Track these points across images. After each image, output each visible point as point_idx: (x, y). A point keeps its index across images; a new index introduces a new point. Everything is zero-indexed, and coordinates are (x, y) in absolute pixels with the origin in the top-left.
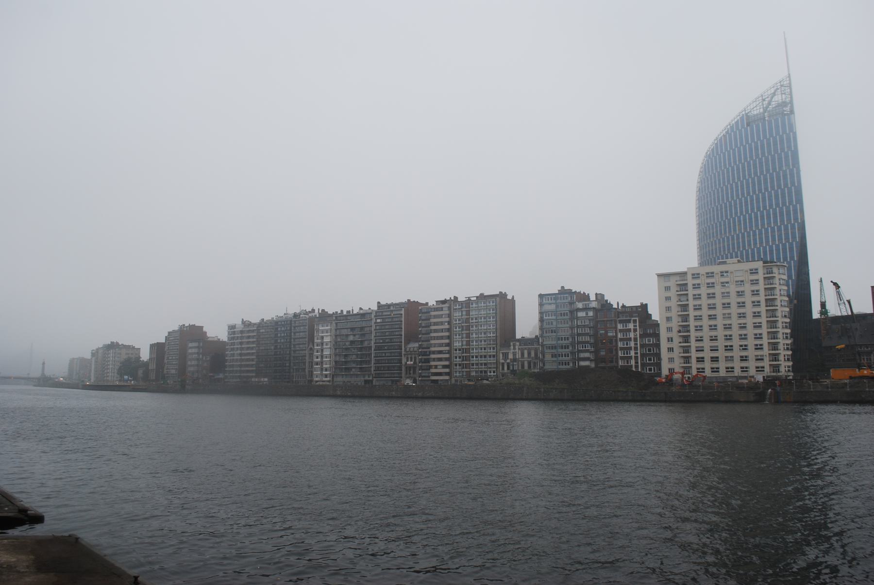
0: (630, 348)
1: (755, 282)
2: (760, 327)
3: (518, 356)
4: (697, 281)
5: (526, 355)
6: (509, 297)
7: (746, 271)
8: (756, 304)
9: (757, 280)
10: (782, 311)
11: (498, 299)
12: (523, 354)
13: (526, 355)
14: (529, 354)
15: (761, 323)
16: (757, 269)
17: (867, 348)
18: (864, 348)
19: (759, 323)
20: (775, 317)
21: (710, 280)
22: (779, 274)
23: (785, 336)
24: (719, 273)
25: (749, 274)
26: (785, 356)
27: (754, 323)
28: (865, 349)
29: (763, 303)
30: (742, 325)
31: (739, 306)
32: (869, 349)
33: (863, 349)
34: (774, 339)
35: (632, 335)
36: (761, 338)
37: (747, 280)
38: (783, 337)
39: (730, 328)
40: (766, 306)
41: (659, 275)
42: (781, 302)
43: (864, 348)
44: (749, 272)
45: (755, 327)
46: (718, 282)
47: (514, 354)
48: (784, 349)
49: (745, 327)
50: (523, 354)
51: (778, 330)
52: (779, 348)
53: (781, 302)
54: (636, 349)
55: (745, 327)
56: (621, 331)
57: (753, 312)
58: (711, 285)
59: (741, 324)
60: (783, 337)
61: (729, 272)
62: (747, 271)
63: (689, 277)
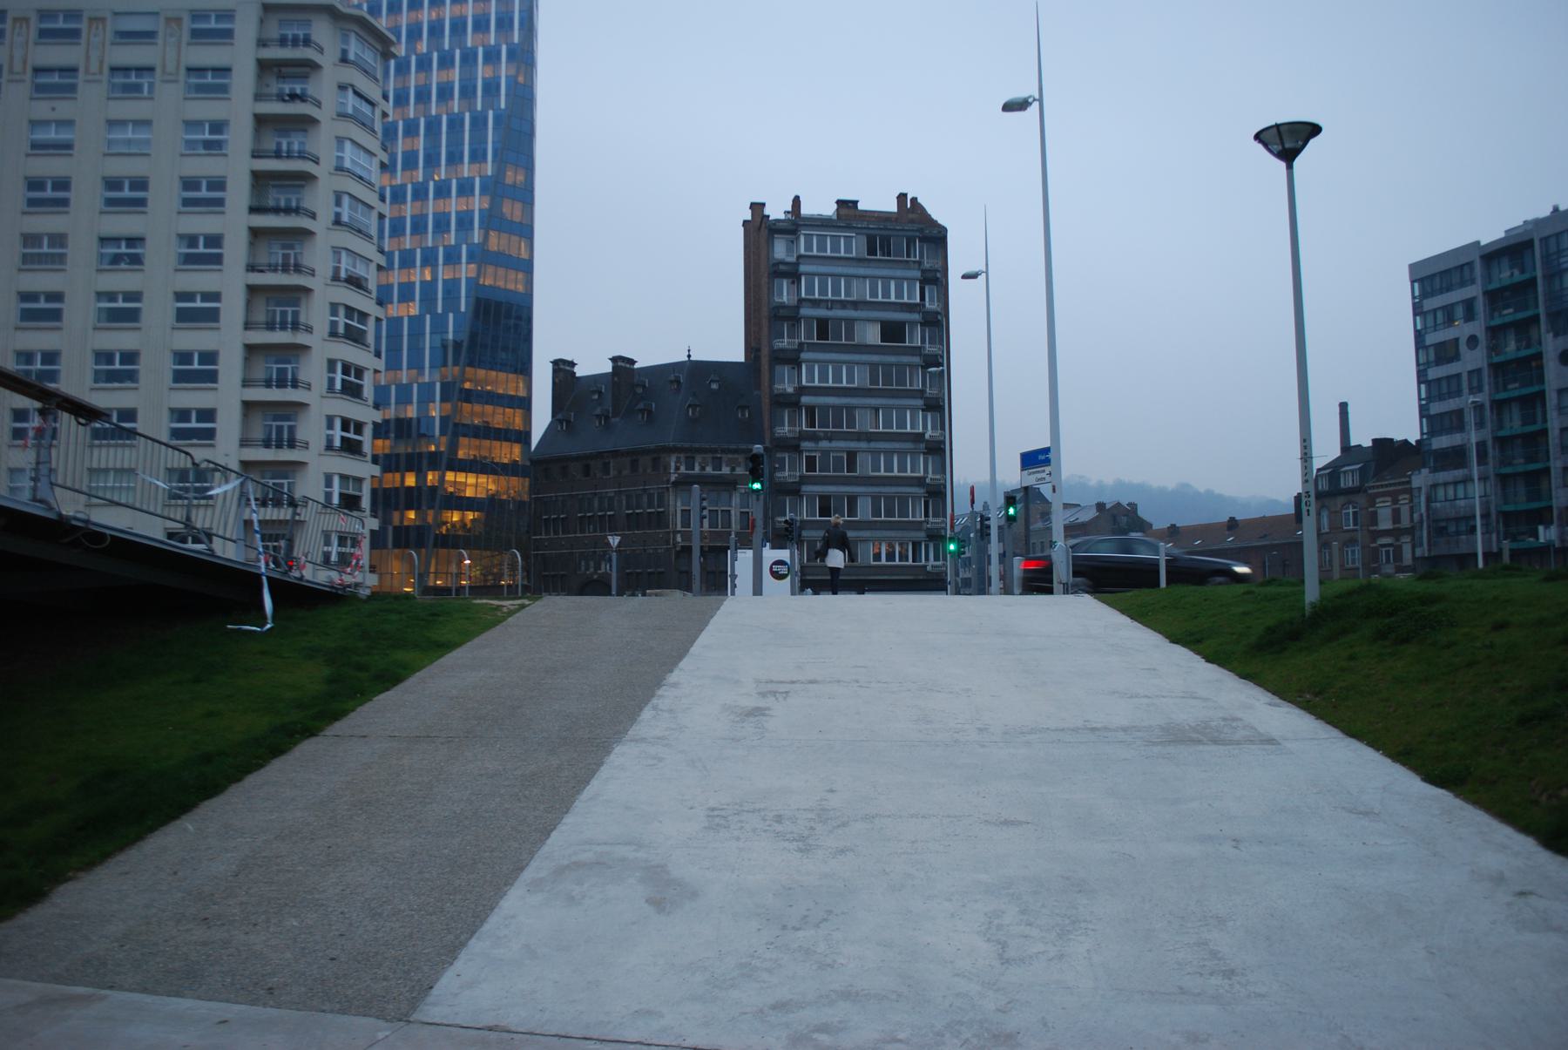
1: (210, 81)
2: (212, 316)
7: (168, 20)
8: (204, 193)
9: (225, 71)
10: (337, 251)
15: (216, 297)
16: (227, 15)
17: (718, 467)
18: (703, 468)
19: (207, 297)
20: (298, 268)
22: (344, 60)
23: (339, 377)
24: (34, 18)
25: (186, 37)
26: (329, 483)
27: (180, 296)
28: (709, 470)
29: (239, 194)
30: (121, 304)
31: (111, 202)
32: (726, 470)
33: (697, 469)
34: (281, 383)
36: (212, 377)
37: (171, 67)
38: (331, 381)
39: (56, 315)
40: (254, 210)
42: (338, 203)
43: (703, 468)
44: (187, 24)
45: (184, 316)
46: (18, 67)
48: (329, 447)
49: (132, 316)
51: (301, 338)
52: (301, 435)
53: (338, 203)
55: (132, 316)
57: (181, 237)
59: (111, 296)
60: (331, 381)
61: (86, 15)
62: (178, 20)
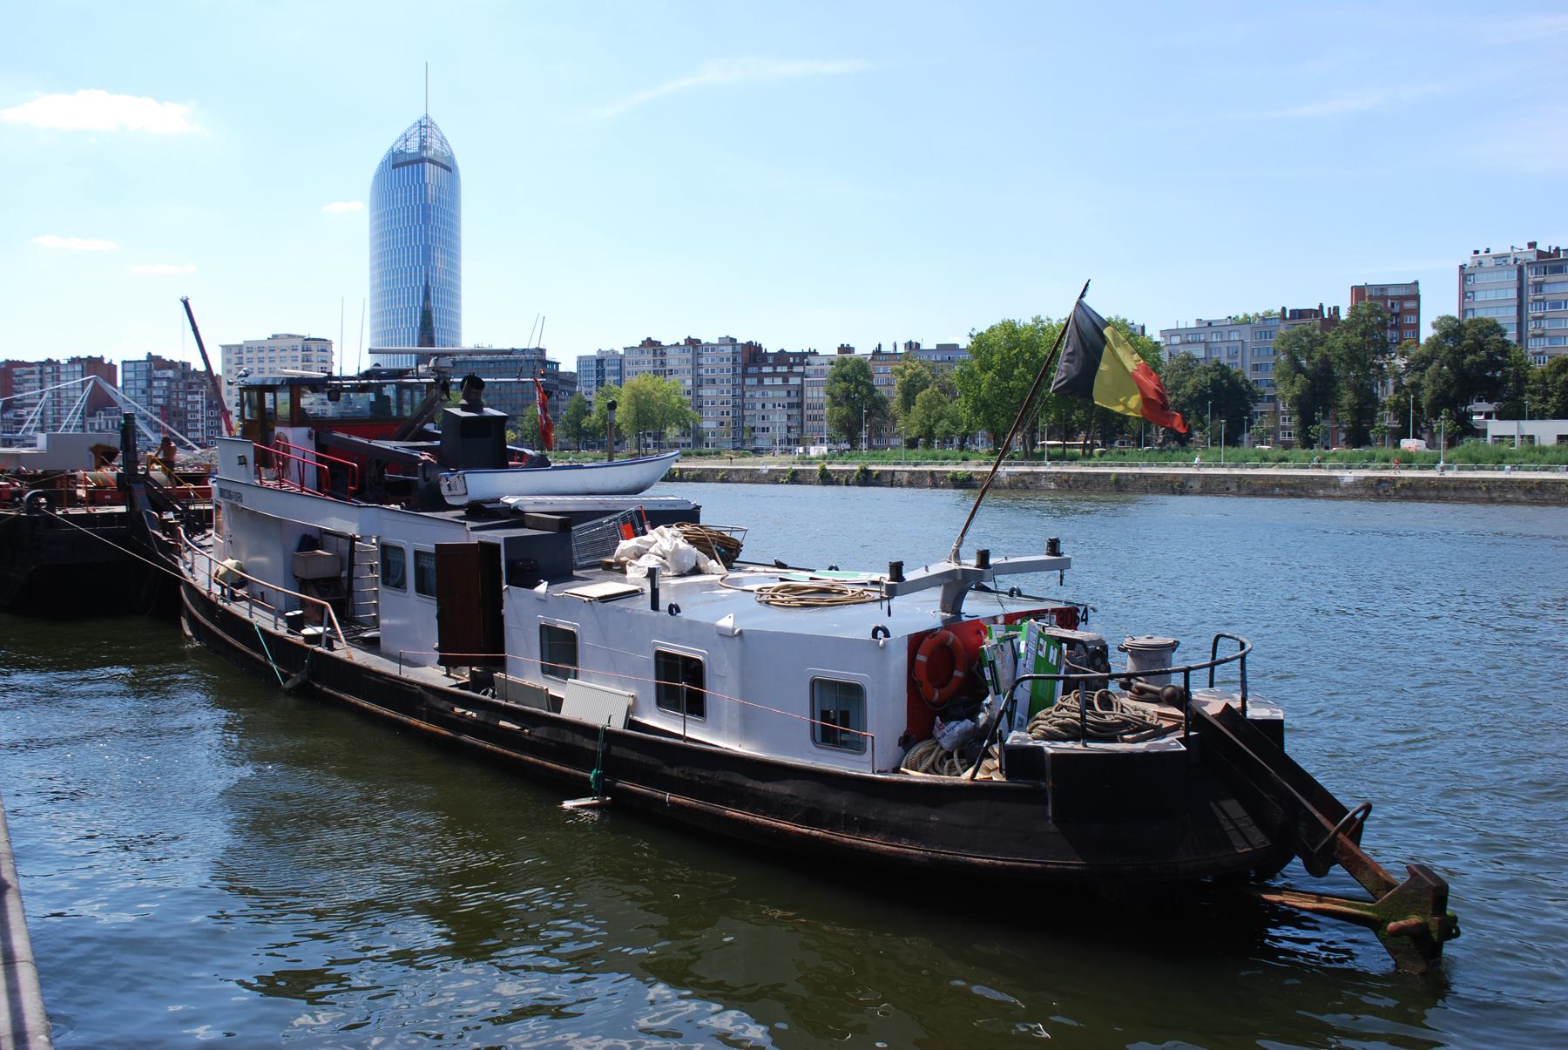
0: (198, 421)
3: (103, 427)
4: (250, 355)
5: (110, 426)
6: (106, 362)
11: (85, 364)
12: (107, 424)
13: (110, 426)
14: (113, 424)
21: (261, 355)
35: (199, 407)
41: (223, 347)
47: (100, 424)
50: (107, 424)
54: (202, 421)
56: (190, 402)
58: (261, 360)
63: (245, 350)
